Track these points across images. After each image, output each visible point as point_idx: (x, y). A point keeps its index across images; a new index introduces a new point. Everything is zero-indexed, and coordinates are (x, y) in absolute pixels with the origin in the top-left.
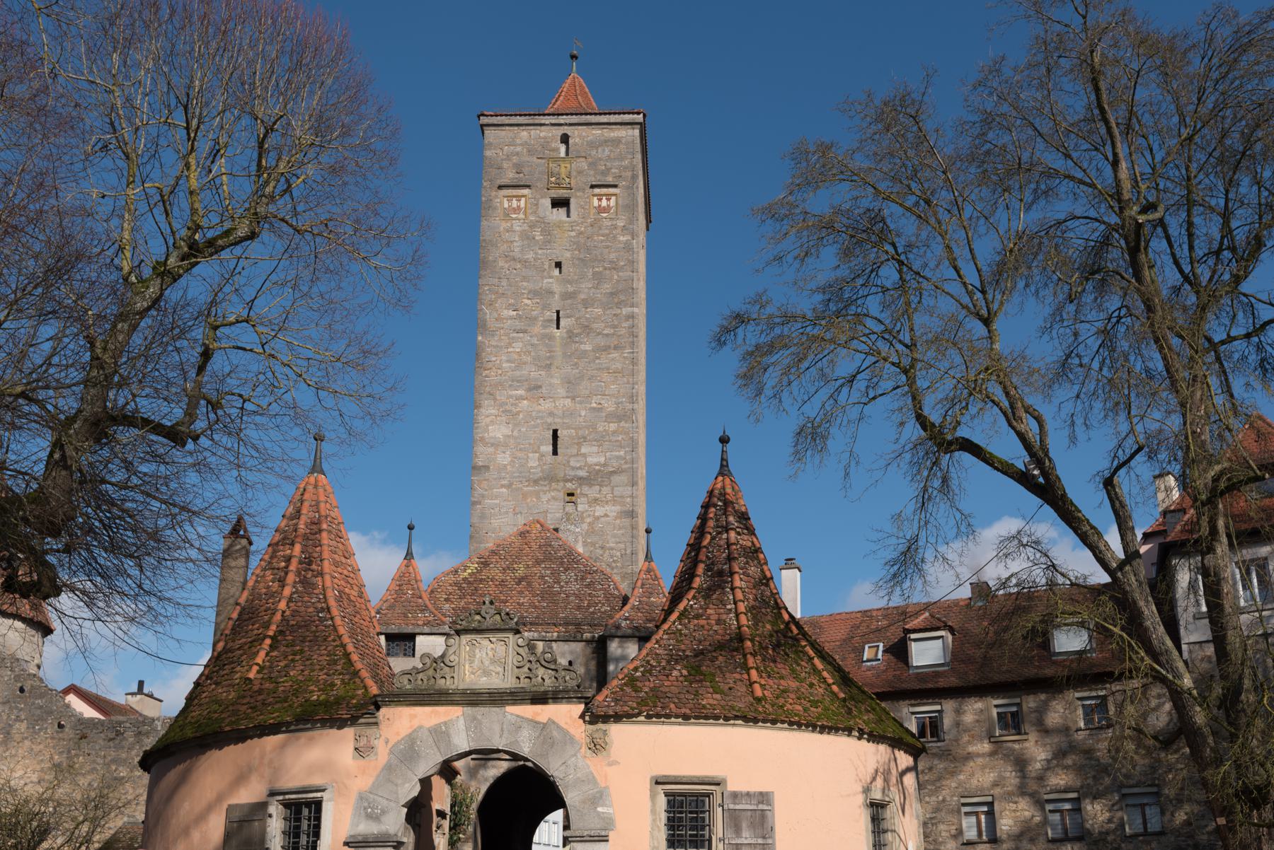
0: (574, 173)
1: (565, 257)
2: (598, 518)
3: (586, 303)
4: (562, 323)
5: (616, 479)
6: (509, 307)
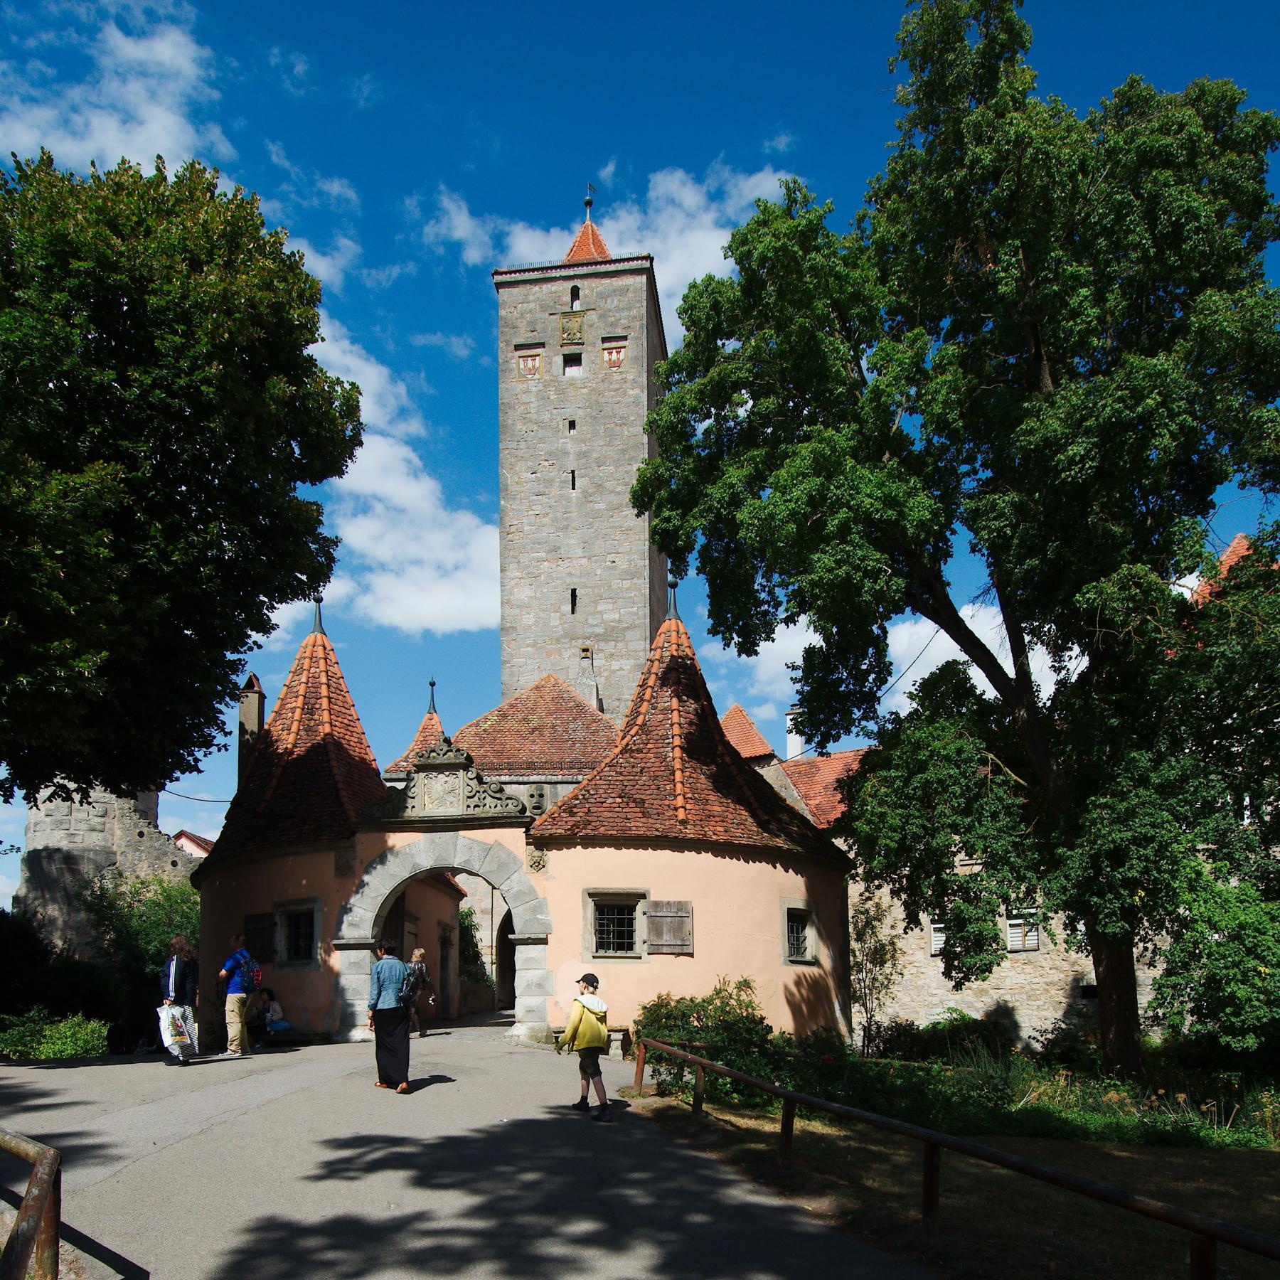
1: (578, 415)
2: (614, 672)
5: (629, 634)
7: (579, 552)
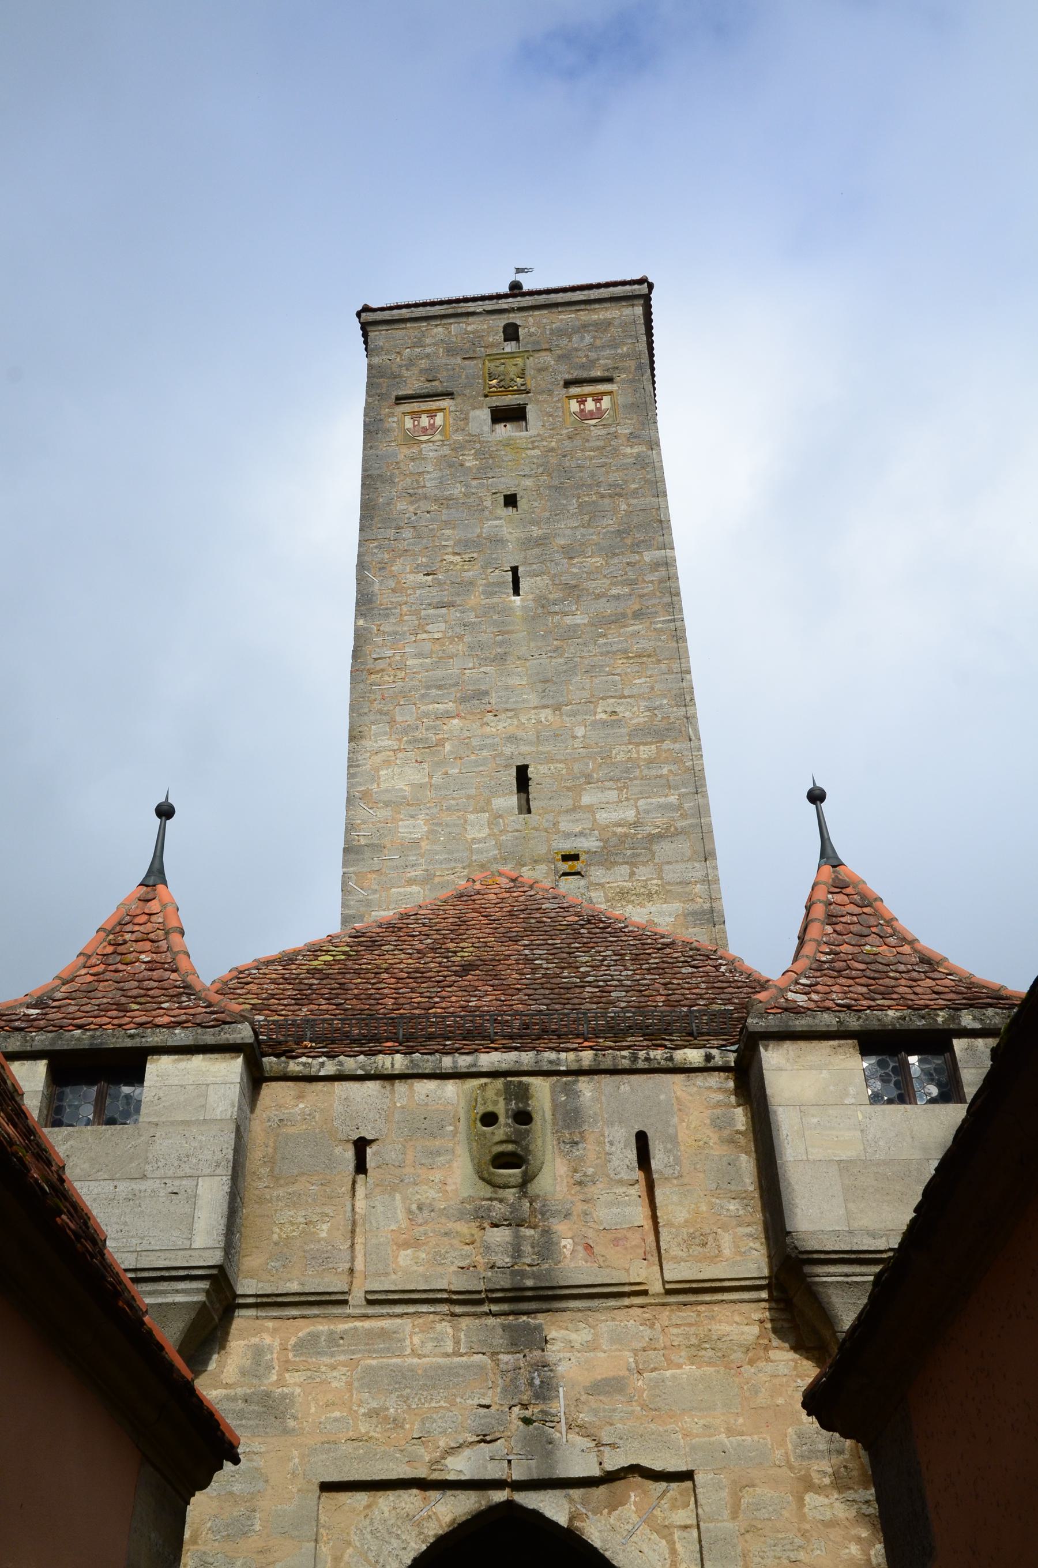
0: (530, 372)
1: (524, 486)
3: (569, 552)
4: (523, 585)
5: (664, 849)
6: (417, 569)
7: (533, 699)
